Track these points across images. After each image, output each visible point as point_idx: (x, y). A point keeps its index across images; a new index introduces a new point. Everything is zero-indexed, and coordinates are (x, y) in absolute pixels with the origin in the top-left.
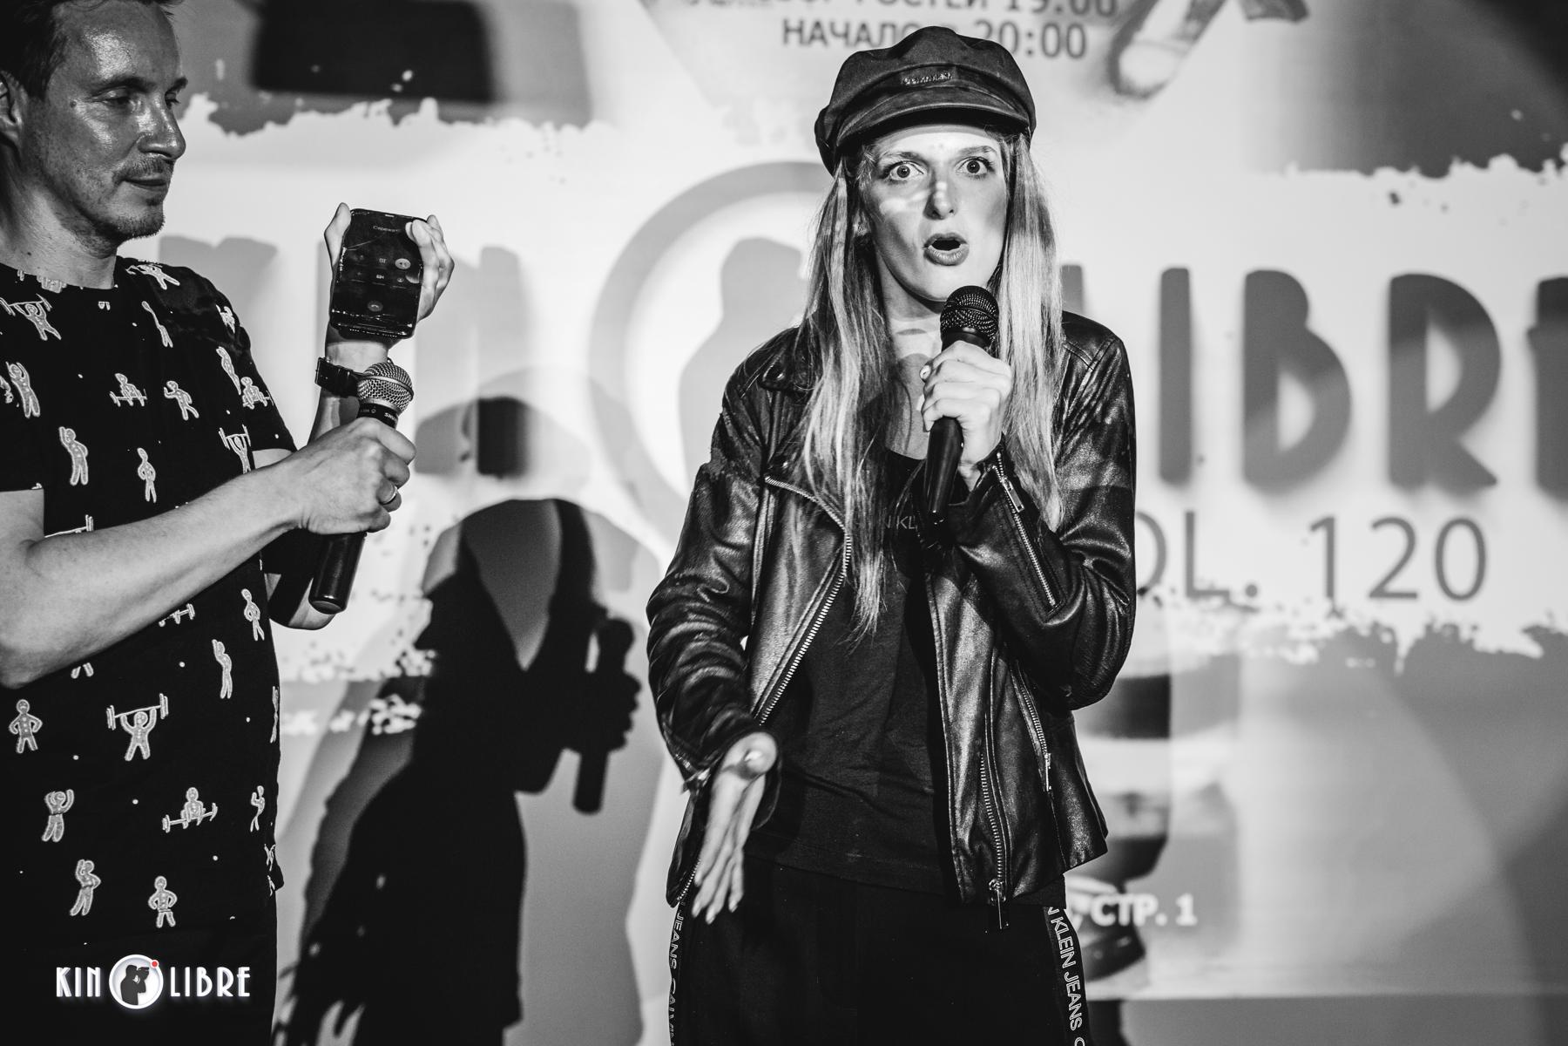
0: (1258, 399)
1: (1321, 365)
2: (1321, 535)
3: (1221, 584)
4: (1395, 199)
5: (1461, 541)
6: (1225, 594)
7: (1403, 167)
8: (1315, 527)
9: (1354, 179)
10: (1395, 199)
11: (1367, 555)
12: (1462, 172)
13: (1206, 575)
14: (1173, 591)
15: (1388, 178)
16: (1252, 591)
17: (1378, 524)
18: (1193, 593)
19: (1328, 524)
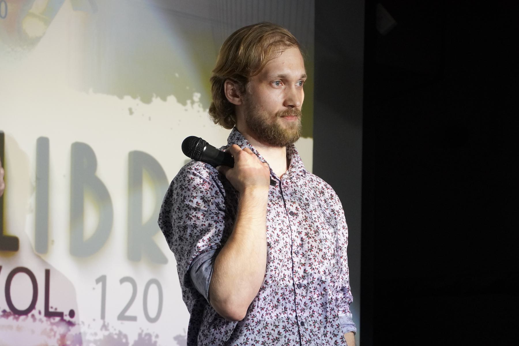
0: (76, 214)
1: (103, 196)
2: (100, 284)
3: (59, 310)
4: (131, 112)
5: (153, 289)
6: (61, 315)
7: (134, 97)
8: (98, 281)
9: (115, 98)
10: (131, 112)
11: (118, 296)
12: (156, 101)
13: (55, 305)
14: (40, 313)
15: (129, 101)
16: (72, 314)
17: (122, 281)
18: (49, 314)
19: (102, 280)
